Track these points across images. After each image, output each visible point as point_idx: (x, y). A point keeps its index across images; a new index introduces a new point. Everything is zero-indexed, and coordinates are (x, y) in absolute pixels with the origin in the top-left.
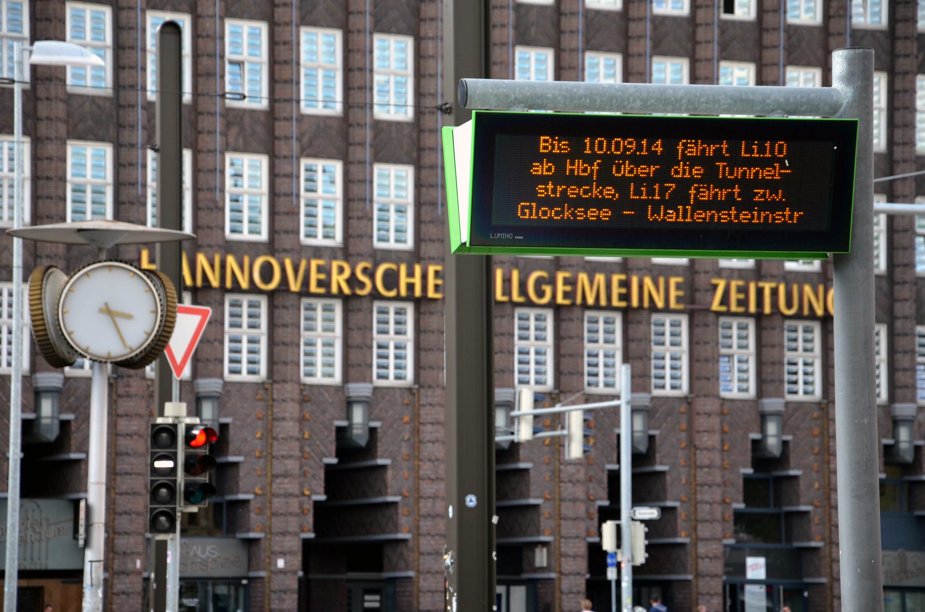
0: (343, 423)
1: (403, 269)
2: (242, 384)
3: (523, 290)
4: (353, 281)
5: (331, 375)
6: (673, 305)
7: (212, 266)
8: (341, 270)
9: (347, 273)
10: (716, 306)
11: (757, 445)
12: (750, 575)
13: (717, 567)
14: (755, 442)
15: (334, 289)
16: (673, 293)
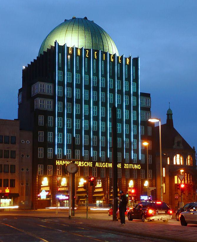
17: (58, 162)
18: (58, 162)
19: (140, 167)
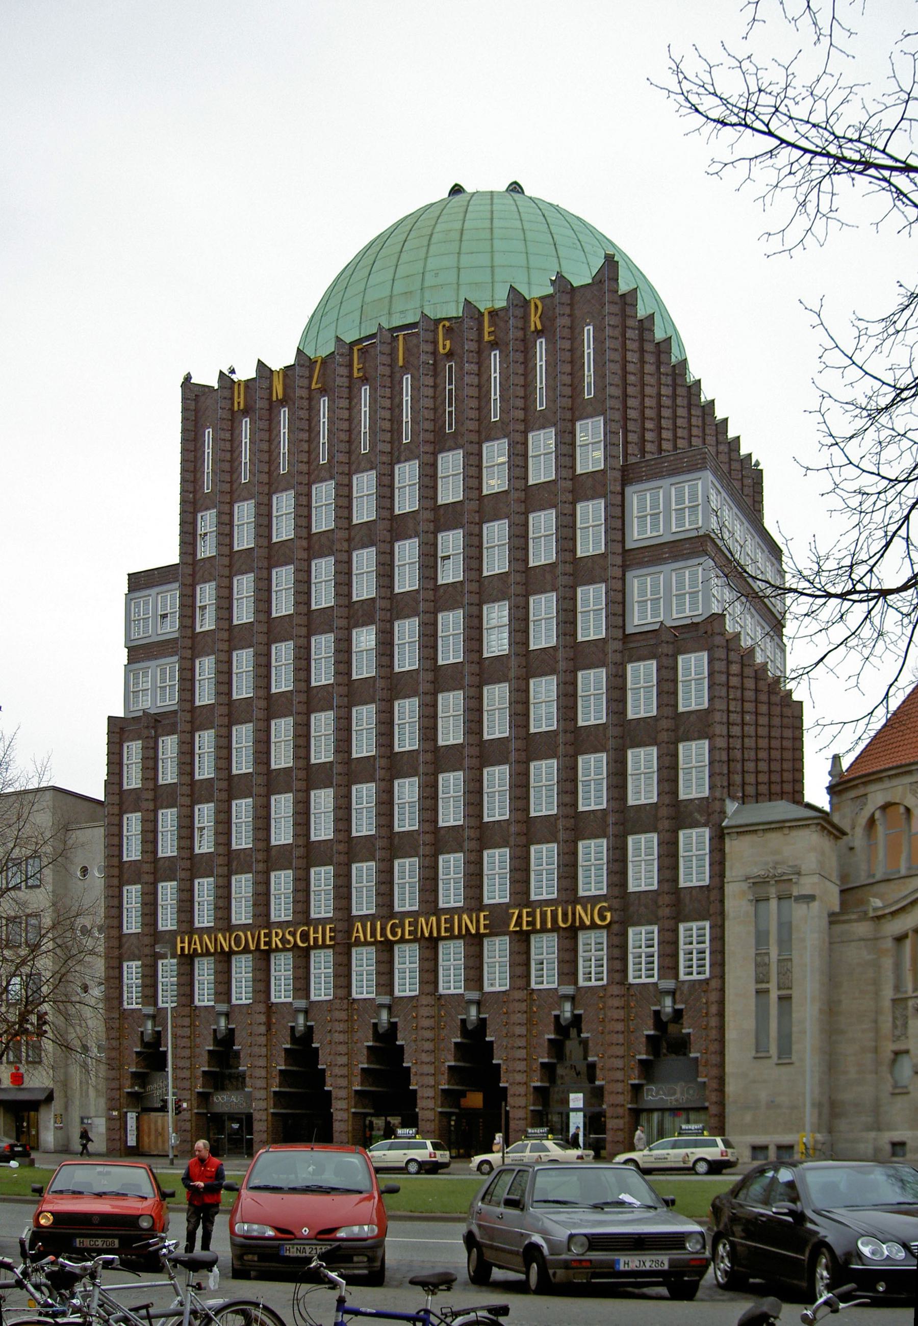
3: (383, 933)
4: (284, 940)
12: (572, 1105)
15: (274, 946)
16: (482, 922)
17: (182, 942)
19: (609, 915)
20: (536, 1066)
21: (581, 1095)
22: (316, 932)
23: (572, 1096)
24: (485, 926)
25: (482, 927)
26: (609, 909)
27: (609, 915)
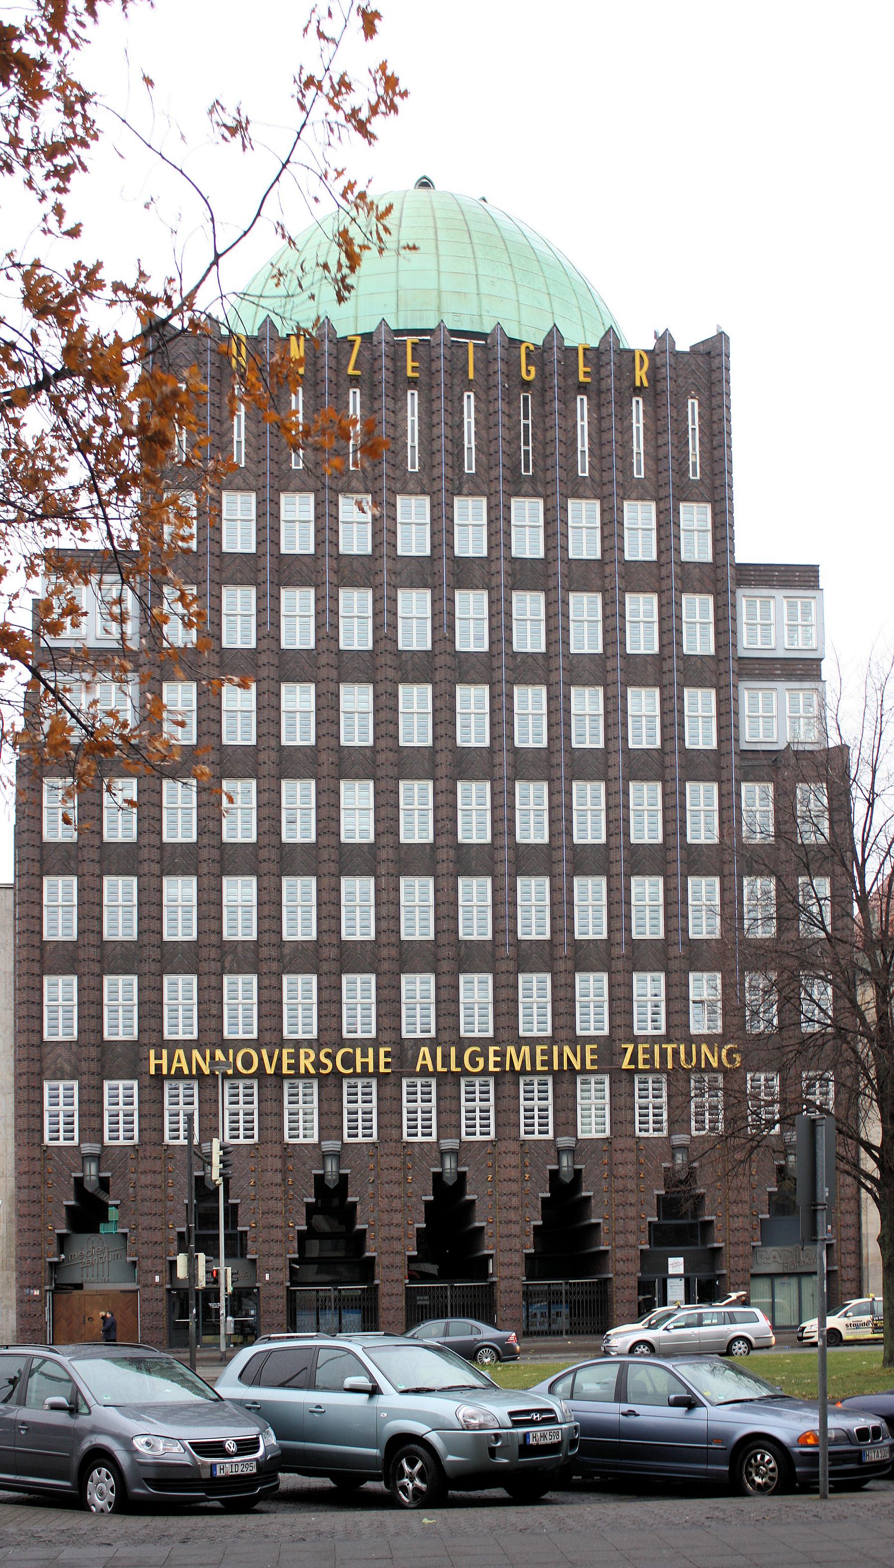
0: (438, 1170)
1: (358, 1051)
2: (59, 1148)
3: (460, 1062)
4: (318, 1064)
5: (132, 1138)
6: (589, 1066)
7: (204, 1059)
8: (307, 1056)
9: (313, 1057)
10: (625, 1065)
11: (554, 1174)
12: (671, 1271)
13: (634, 1267)
14: (552, 1172)
15: (302, 1071)
16: (589, 1057)
17: (158, 1057)
18: (158, 1057)
19: (737, 1057)
20: (644, 1226)
21: (681, 1260)
22: (365, 1055)
23: (671, 1260)
24: (593, 1062)
25: (588, 1062)
26: (737, 1051)
27: (737, 1057)
